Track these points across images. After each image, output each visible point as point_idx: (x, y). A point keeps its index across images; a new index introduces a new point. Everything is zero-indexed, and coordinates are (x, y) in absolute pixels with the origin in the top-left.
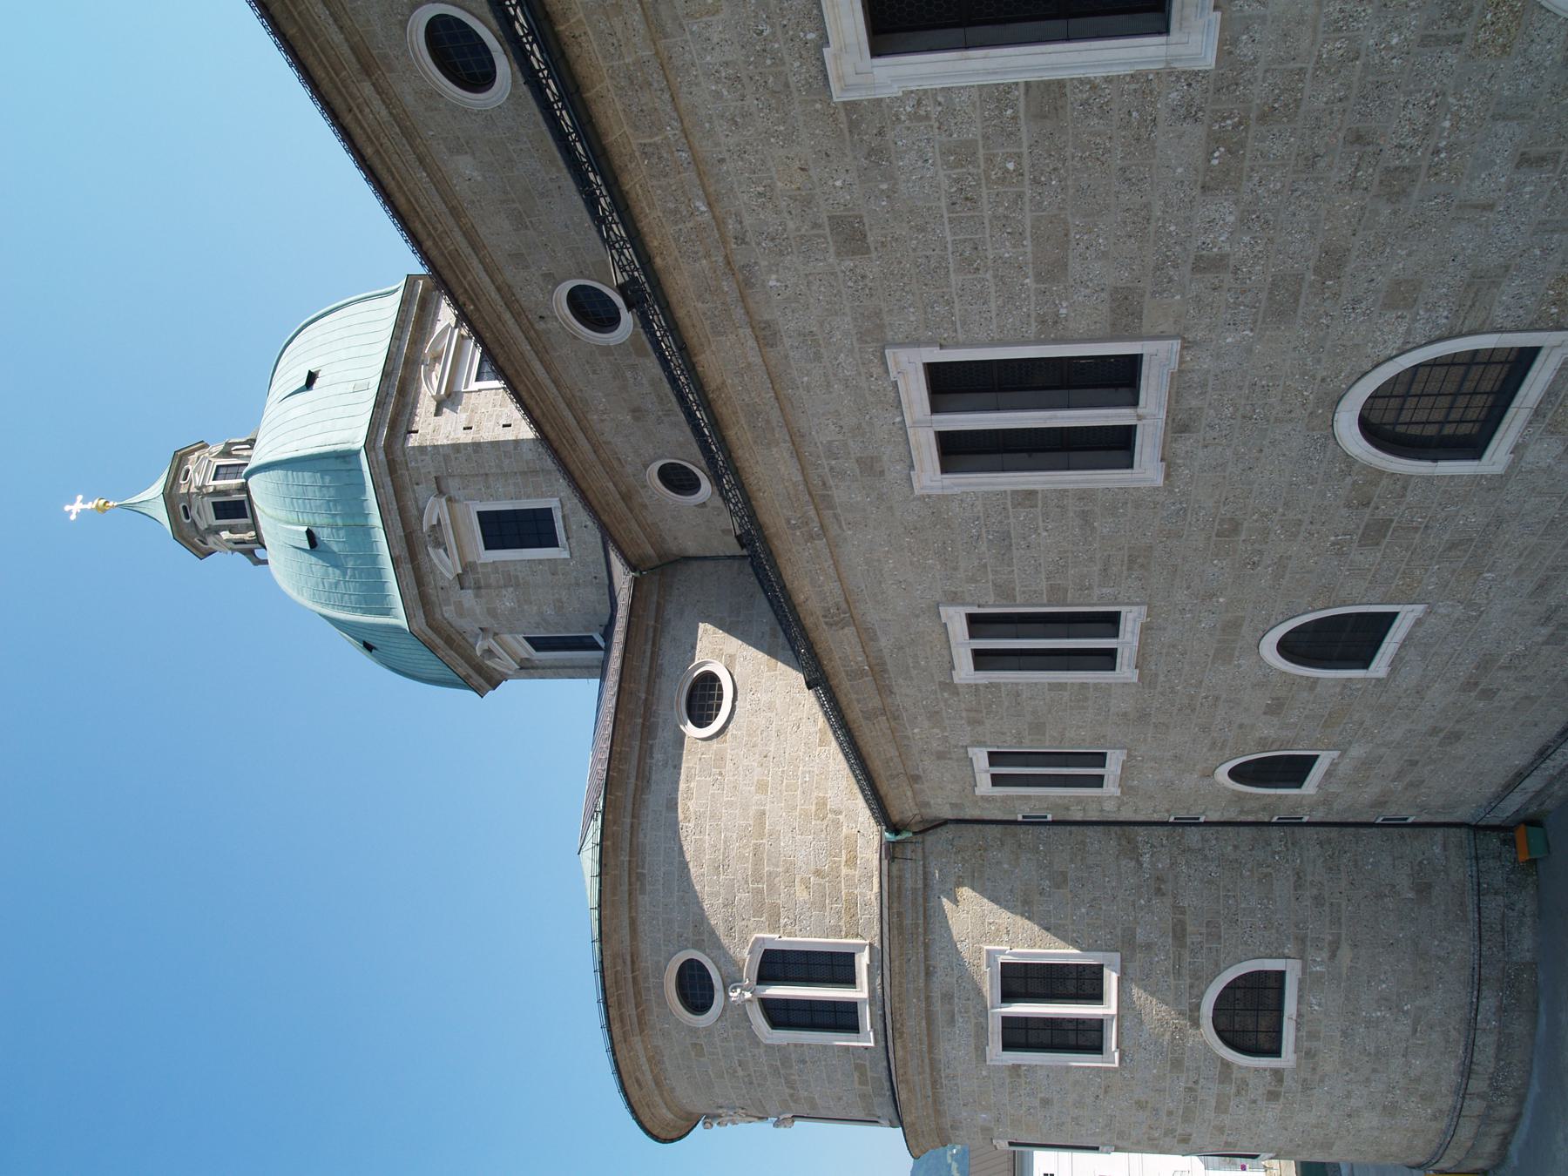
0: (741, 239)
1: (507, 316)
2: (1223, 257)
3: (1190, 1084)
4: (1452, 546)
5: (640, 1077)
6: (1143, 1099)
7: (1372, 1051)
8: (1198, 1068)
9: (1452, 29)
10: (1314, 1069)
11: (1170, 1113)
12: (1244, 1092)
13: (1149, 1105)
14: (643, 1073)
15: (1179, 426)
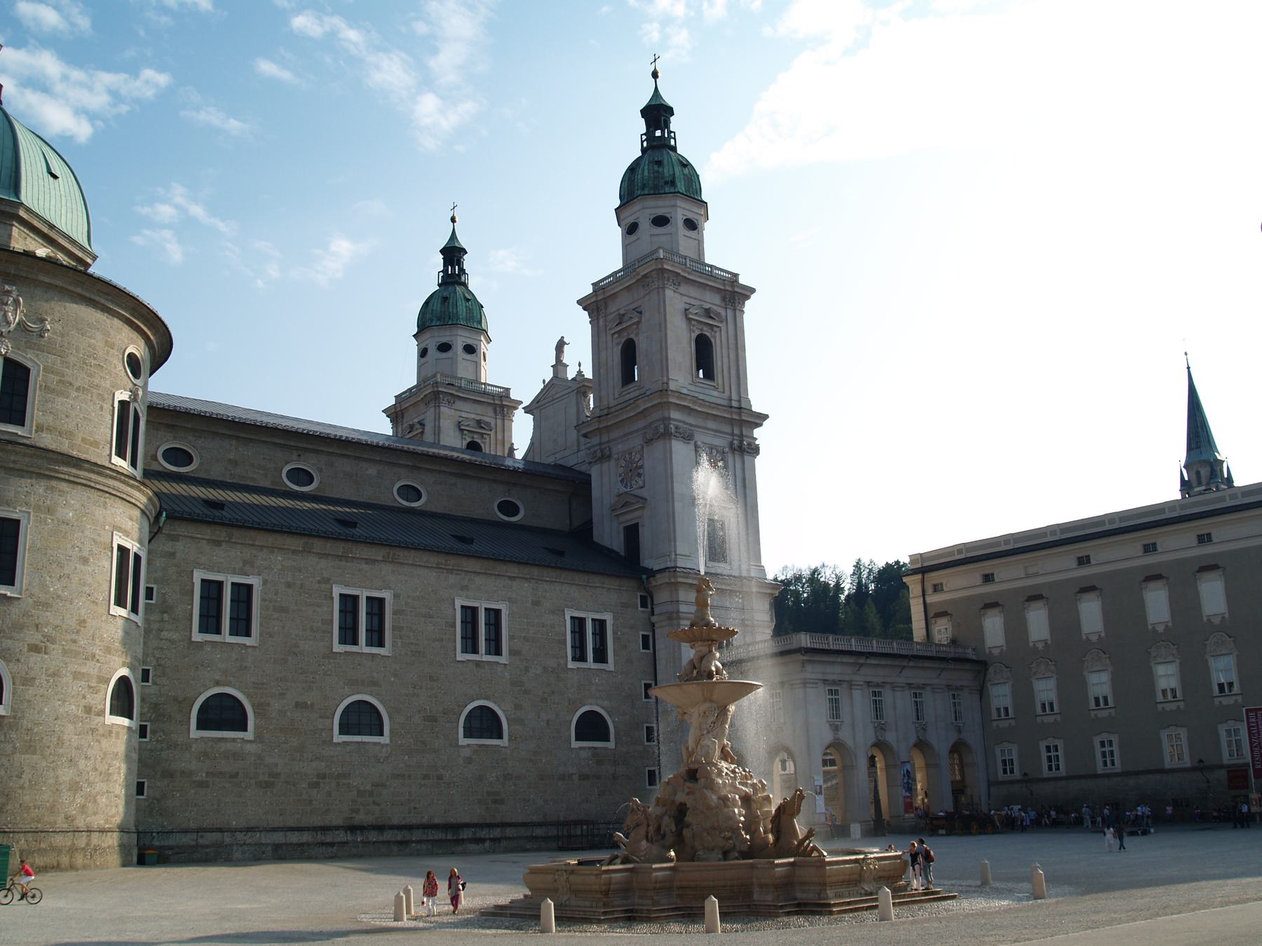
0: (536, 583)
1: (311, 446)
2: (529, 671)
3: (97, 657)
4: (423, 742)
5: (106, 296)
6: (87, 625)
7: (110, 771)
8: (106, 663)
9: (571, 702)
10: (103, 735)
11: (75, 642)
12: (91, 691)
13: (82, 629)
14: (107, 299)
15: (478, 664)
